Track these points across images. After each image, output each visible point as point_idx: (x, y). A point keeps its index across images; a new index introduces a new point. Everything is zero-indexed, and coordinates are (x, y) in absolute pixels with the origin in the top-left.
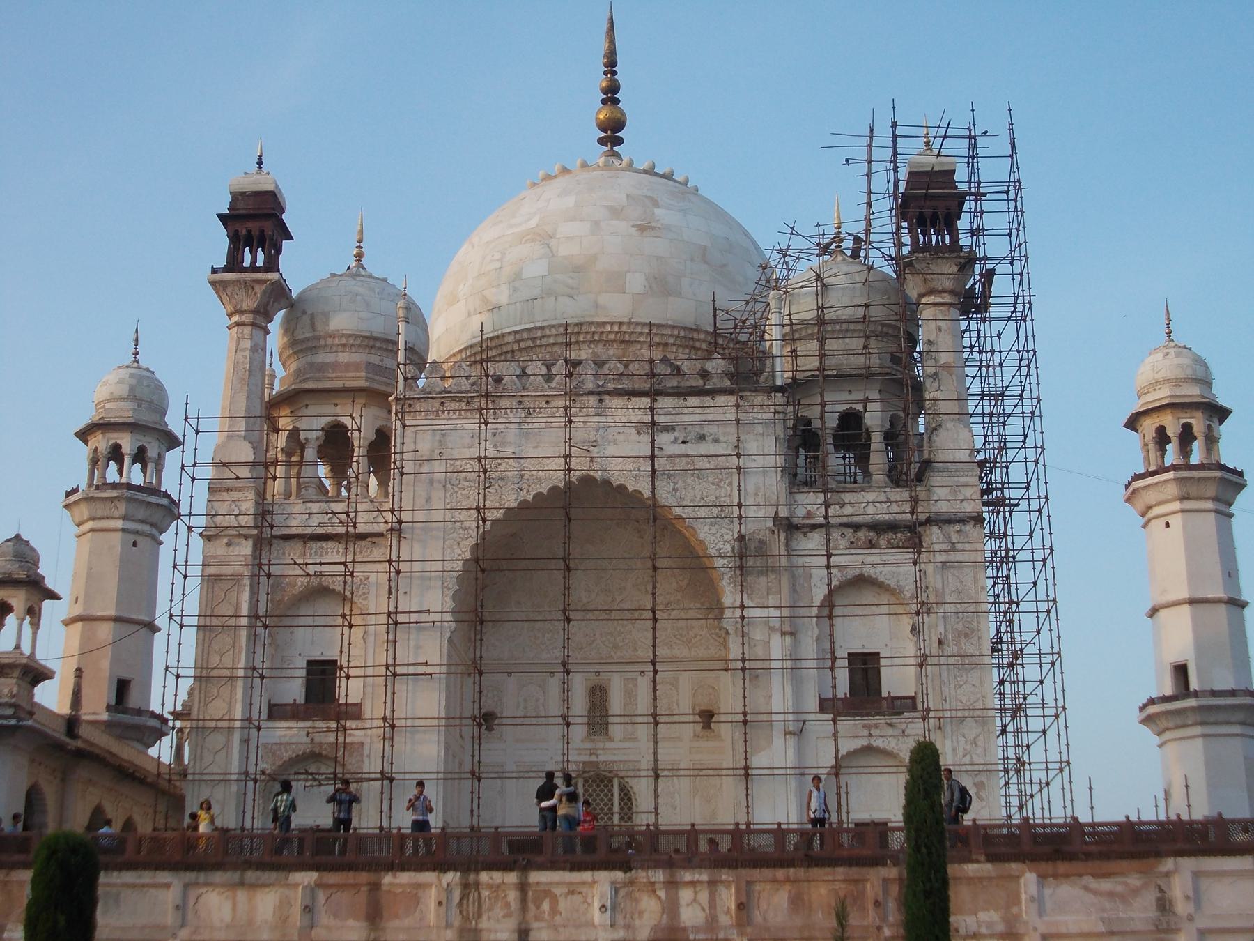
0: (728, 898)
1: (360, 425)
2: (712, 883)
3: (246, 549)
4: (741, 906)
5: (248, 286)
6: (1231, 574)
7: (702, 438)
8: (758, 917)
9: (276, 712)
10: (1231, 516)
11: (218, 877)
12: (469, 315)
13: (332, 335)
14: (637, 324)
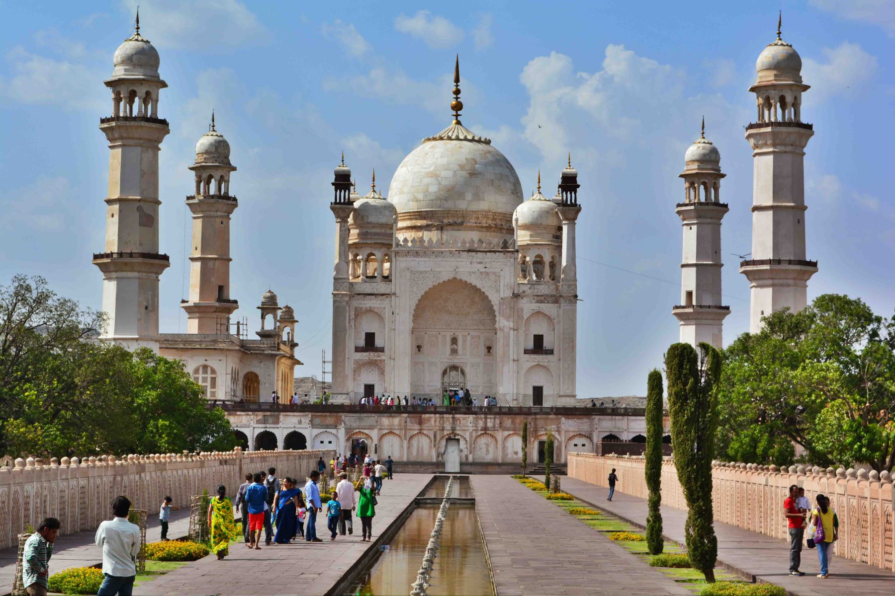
0: (498, 421)
3: (347, 299)
5: (344, 210)
9: (358, 349)
13: (368, 223)
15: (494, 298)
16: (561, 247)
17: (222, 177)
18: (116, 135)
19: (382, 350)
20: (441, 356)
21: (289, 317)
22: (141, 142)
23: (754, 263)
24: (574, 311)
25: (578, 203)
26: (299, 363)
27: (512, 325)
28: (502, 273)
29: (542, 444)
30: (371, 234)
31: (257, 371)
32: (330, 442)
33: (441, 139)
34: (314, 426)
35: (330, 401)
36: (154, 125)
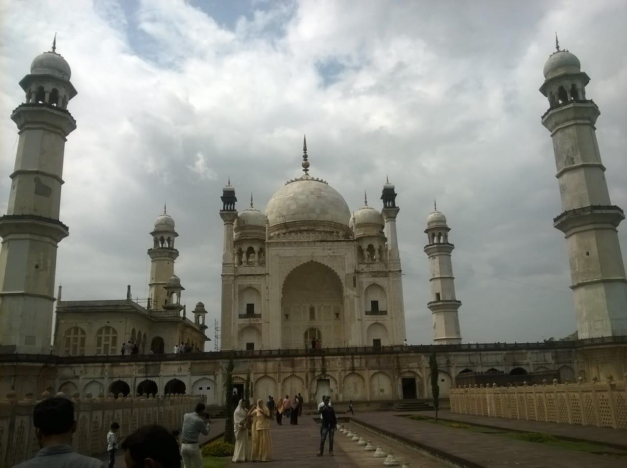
0: (364, 361)
1: (256, 248)
2: (361, 358)
4: (366, 363)
6: (450, 271)
9: (241, 316)
10: (451, 256)
11: (260, 359)
12: (276, 217)
14: (319, 221)
15: (342, 275)
16: (386, 239)
17: (169, 238)
18: (23, 121)
20: (302, 322)
21: (200, 310)
22: (44, 126)
24: (400, 282)
25: (396, 206)
27: (355, 294)
28: (346, 256)
29: (404, 380)
30: (250, 233)
32: (209, 388)
33: (297, 180)
34: (192, 374)
36: (56, 112)
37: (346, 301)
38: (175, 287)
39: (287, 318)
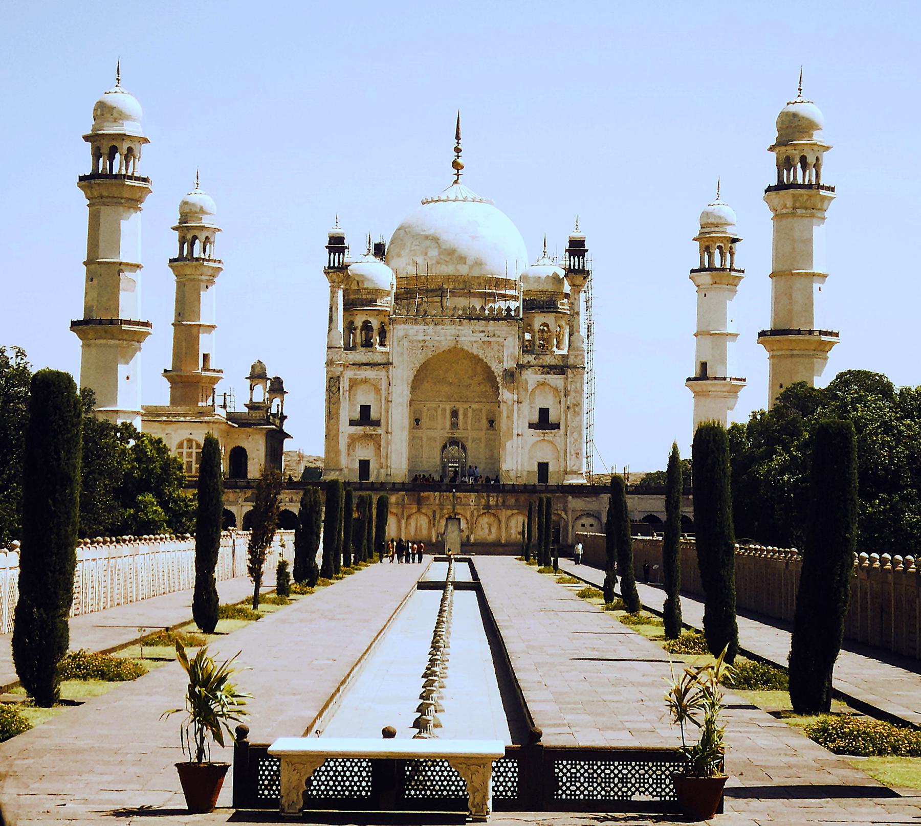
0: (501, 500)
1: (375, 324)
2: (497, 497)
3: (341, 369)
7: (494, 335)
8: (507, 503)
9: (352, 423)
15: (497, 369)
17: (207, 238)
18: (96, 194)
19: (377, 423)
20: (440, 429)
21: (277, 388)
23: (773, 332)
26: (288, 436)
27: (516, 399)
31: (244, 445)
35: (566, 482)
37: (503, 407)
38: (257, 375)
39: (417, 424)
